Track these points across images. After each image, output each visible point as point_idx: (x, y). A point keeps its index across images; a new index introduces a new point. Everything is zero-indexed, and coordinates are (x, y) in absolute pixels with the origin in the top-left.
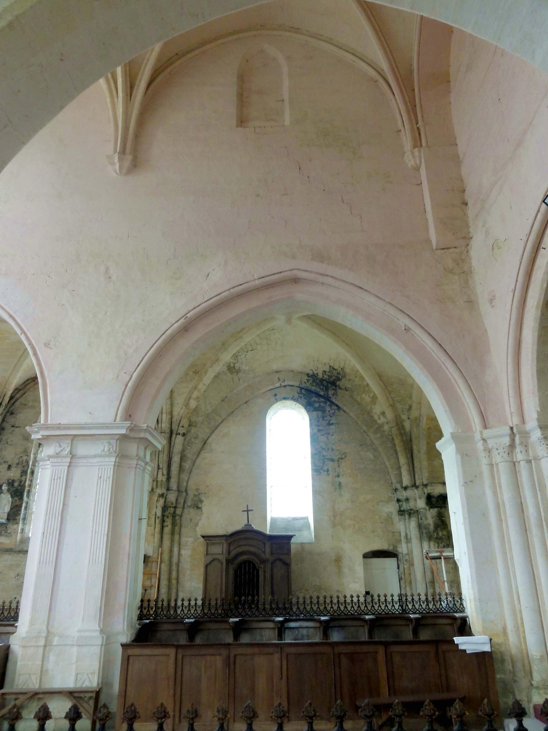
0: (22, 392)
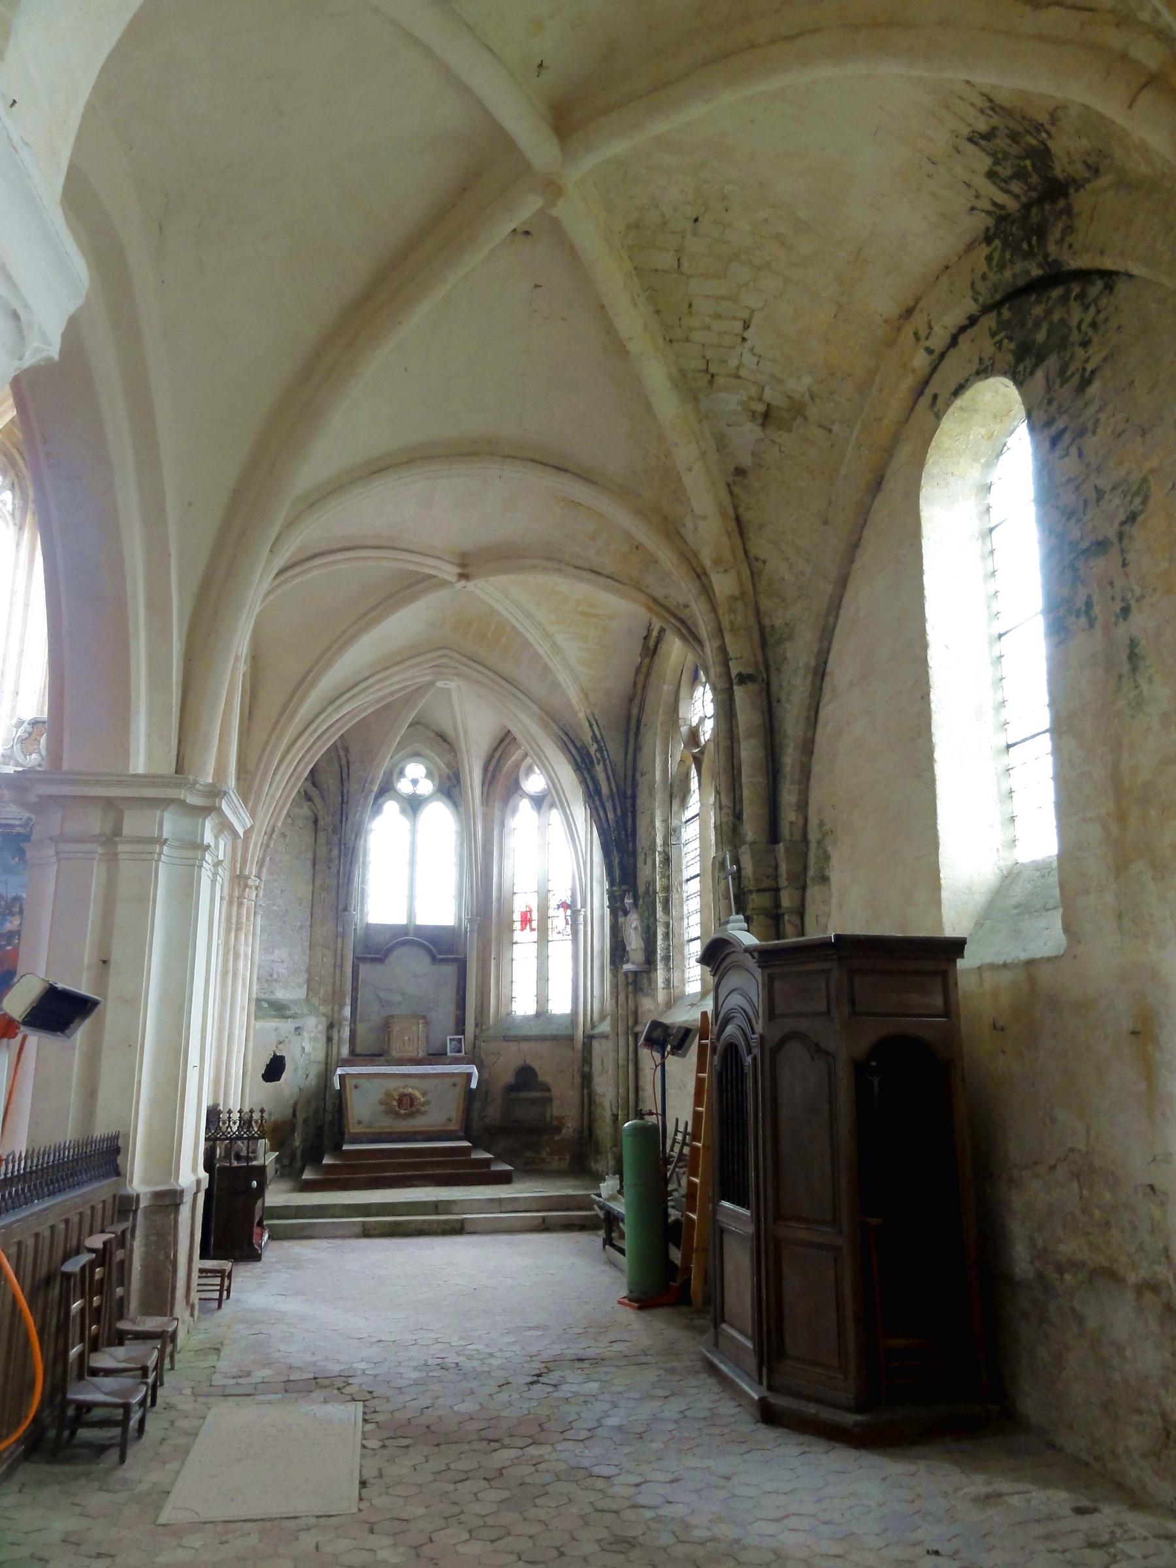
0: (637, 702)
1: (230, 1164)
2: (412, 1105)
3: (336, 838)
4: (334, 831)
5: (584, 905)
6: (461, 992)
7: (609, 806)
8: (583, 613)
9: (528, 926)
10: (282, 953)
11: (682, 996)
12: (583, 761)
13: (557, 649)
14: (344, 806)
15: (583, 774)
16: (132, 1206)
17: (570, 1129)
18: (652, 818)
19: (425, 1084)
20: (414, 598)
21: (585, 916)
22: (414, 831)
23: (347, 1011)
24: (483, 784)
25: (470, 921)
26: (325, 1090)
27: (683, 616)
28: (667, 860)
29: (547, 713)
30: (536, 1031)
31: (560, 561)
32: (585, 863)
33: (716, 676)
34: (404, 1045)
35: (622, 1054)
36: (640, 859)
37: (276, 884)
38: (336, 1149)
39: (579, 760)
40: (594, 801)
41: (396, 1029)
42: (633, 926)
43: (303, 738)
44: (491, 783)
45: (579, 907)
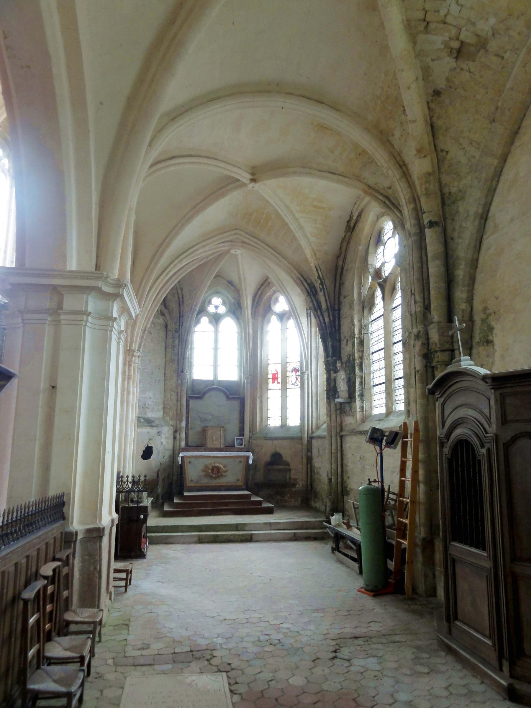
0: (342, 258)
1: (128, 505)
2: (218, 472)
3: (177, 335)
4: (176, 331)
5: (307, 370)
6: (242, 414)
7: (326, 314)
8: (315, 206)
9: (276, 381)
10: (150, 394)
11: (371, 415)
12: (311, 291)
13: (301, 227)
14: (181, 319)
15: (311, 298)
16: (73, 538)
17: (300, 485)
18: (352, 320)
19: (225, 461)
20: (223, 195)
21: (308, 375)
22: (216, 332)
23: (184, 424)
24: (252, 308)
25: (246, 378)
26: (173, 464)
27: (387, 194)
28: (361, 342)
29: (292, 265)
30: (281, 435)
31: (311, 168)
32: (307, 347)
33: (411, 226)
34: (213, 442)
35: (334, 447)
36: (344, 343)
37: (147, 358)
38: (180, 494)
39: (309, 290)
40: (317, 313)
41: (209, 433)
42: (342, 378)
43: (162, 277)
44: (256, 308)
45: (304, 370)
